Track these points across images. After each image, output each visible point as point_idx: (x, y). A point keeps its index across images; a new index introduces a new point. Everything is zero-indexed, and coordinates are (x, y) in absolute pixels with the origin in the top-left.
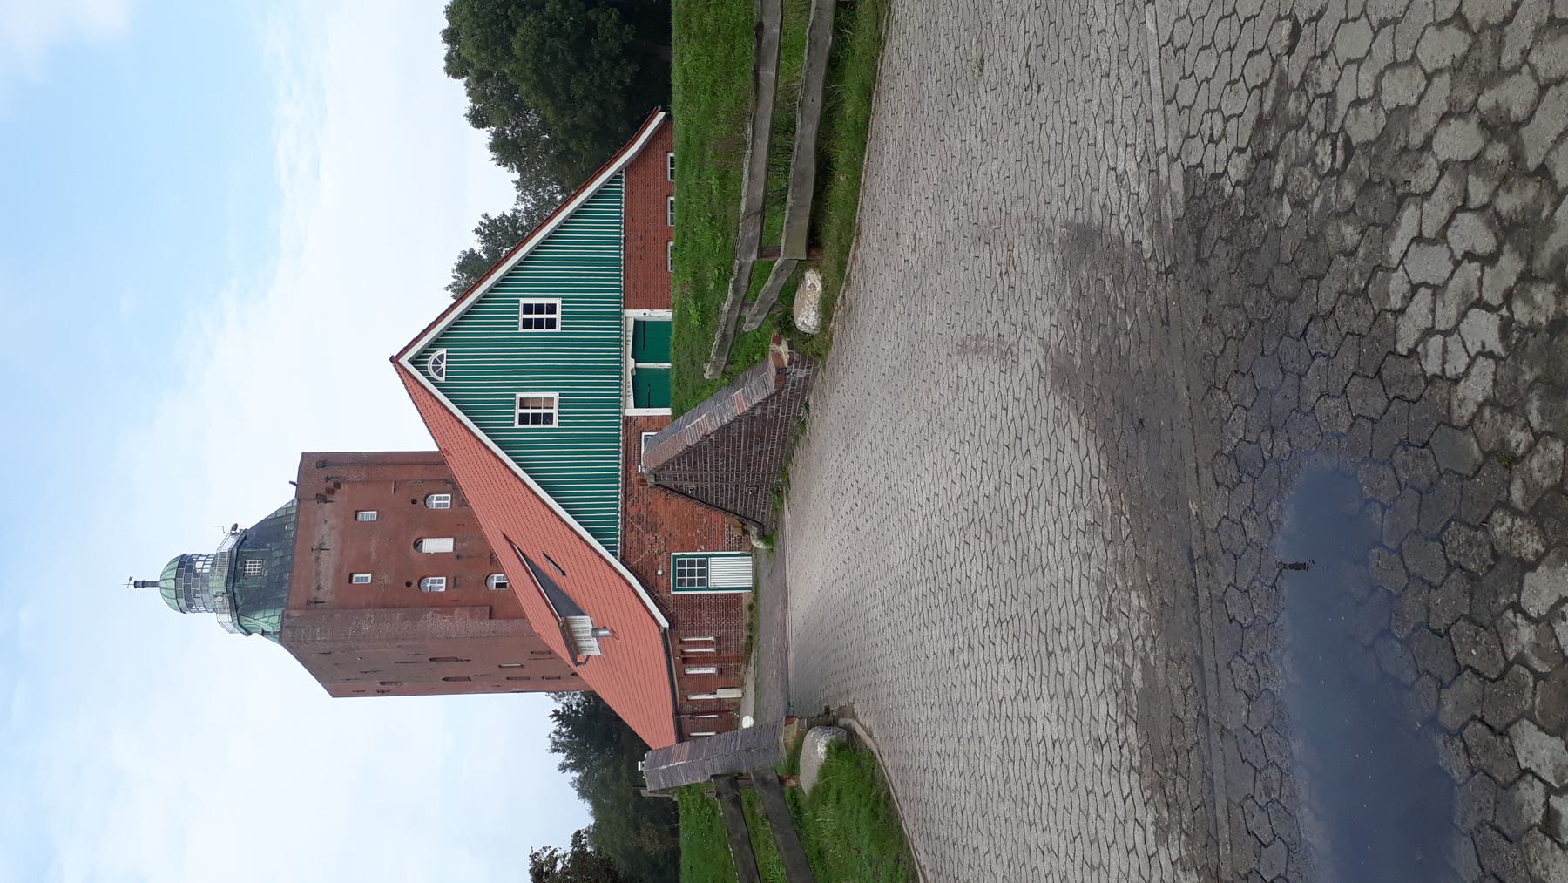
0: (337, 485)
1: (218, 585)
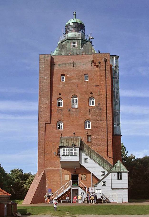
0: (97, 66)
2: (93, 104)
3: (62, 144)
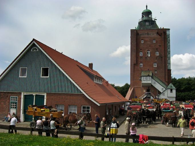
0: (160, 35)
1: (145, 18)
2: (158, 55)
3: (143, 74)
